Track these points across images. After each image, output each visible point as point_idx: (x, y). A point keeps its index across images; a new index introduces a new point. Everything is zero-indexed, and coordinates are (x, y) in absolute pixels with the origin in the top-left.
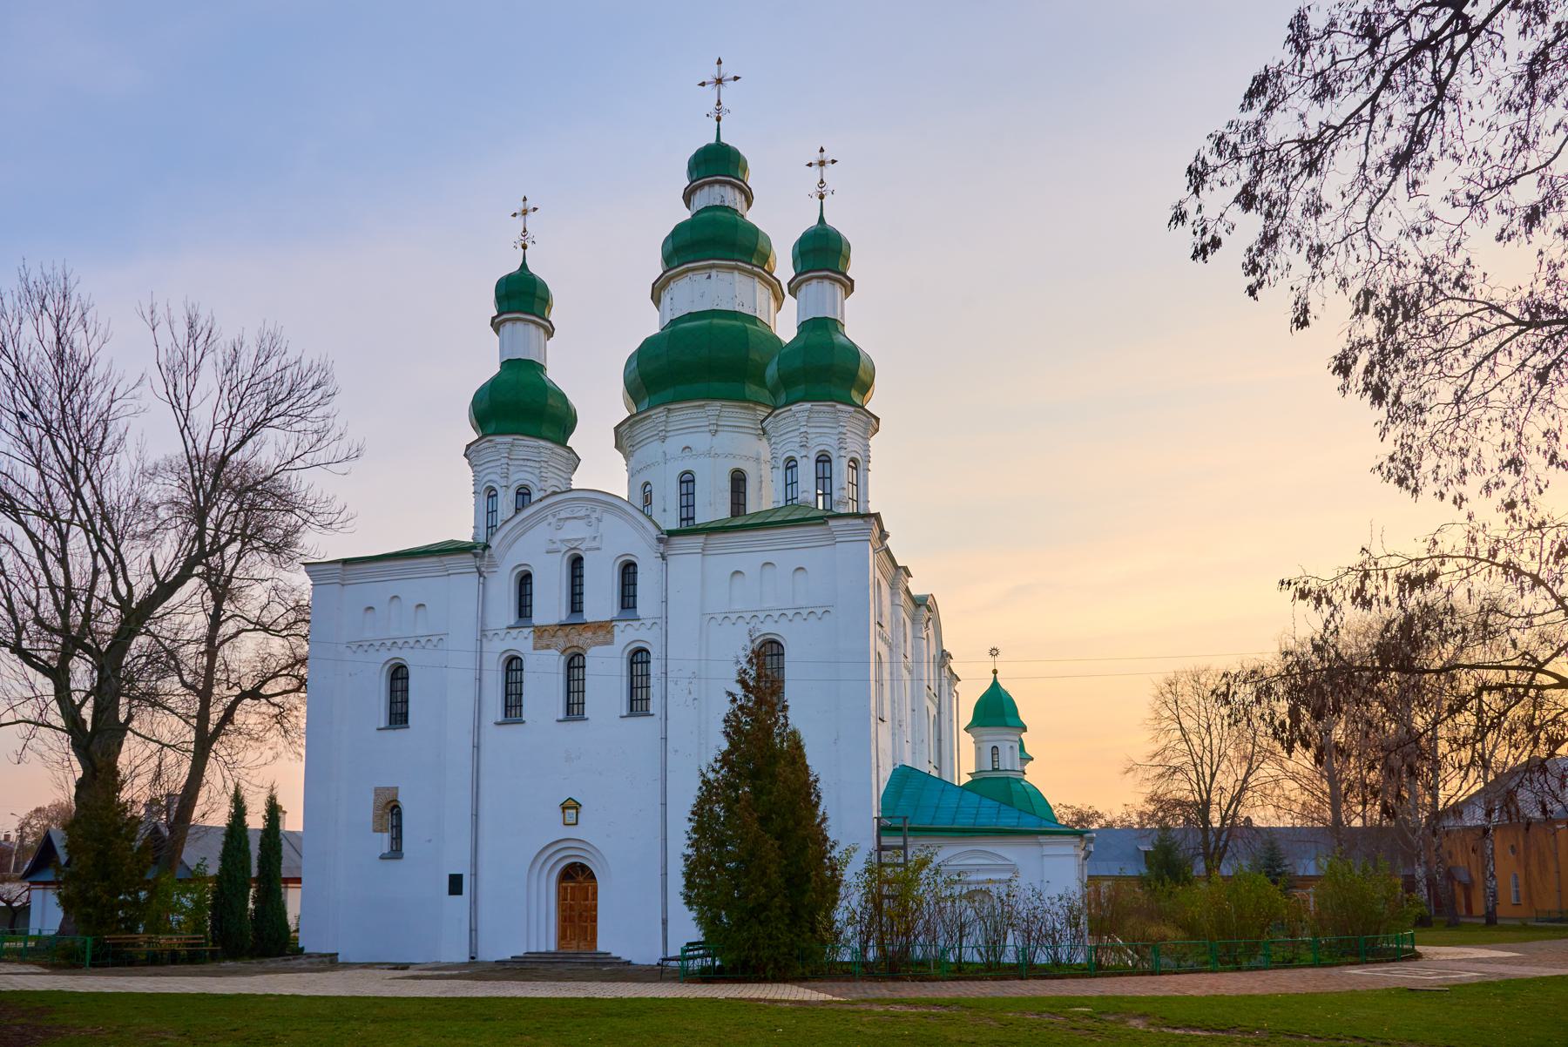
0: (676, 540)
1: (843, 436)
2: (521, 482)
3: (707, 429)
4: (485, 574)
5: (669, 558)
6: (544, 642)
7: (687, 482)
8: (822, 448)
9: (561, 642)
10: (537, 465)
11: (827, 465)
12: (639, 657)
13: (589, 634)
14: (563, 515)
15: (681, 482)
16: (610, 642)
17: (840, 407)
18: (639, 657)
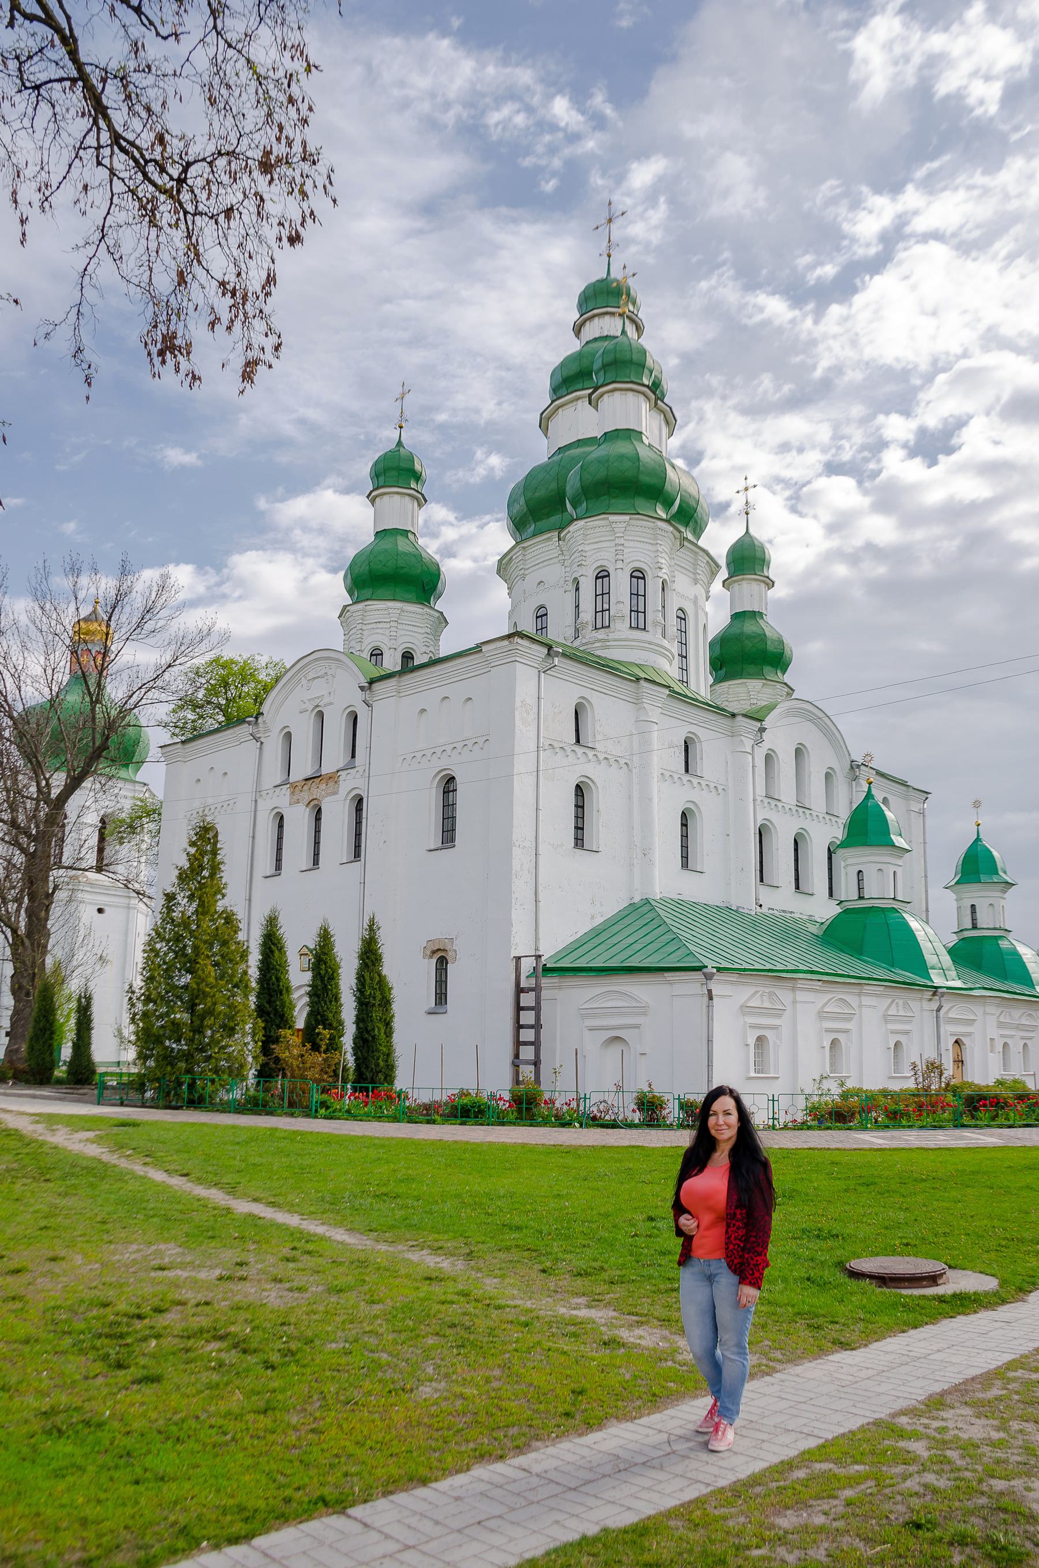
0: (376, 686)
1: (621, 548)
2: (372, 645)
3: (556, 560)
4: (262, 740)
5: (374, 704)
6: (296, 797)
7: (541, 616)
8: (599, 564)
9: (306, 796)
10: (388, 625)
11: (606, 580)
12: (359, 804)
13: (323, 786)
14: (311, 676)
15: (537, 617)
16: (335, 793)
17: (612, 518)
18: (359, 804)
